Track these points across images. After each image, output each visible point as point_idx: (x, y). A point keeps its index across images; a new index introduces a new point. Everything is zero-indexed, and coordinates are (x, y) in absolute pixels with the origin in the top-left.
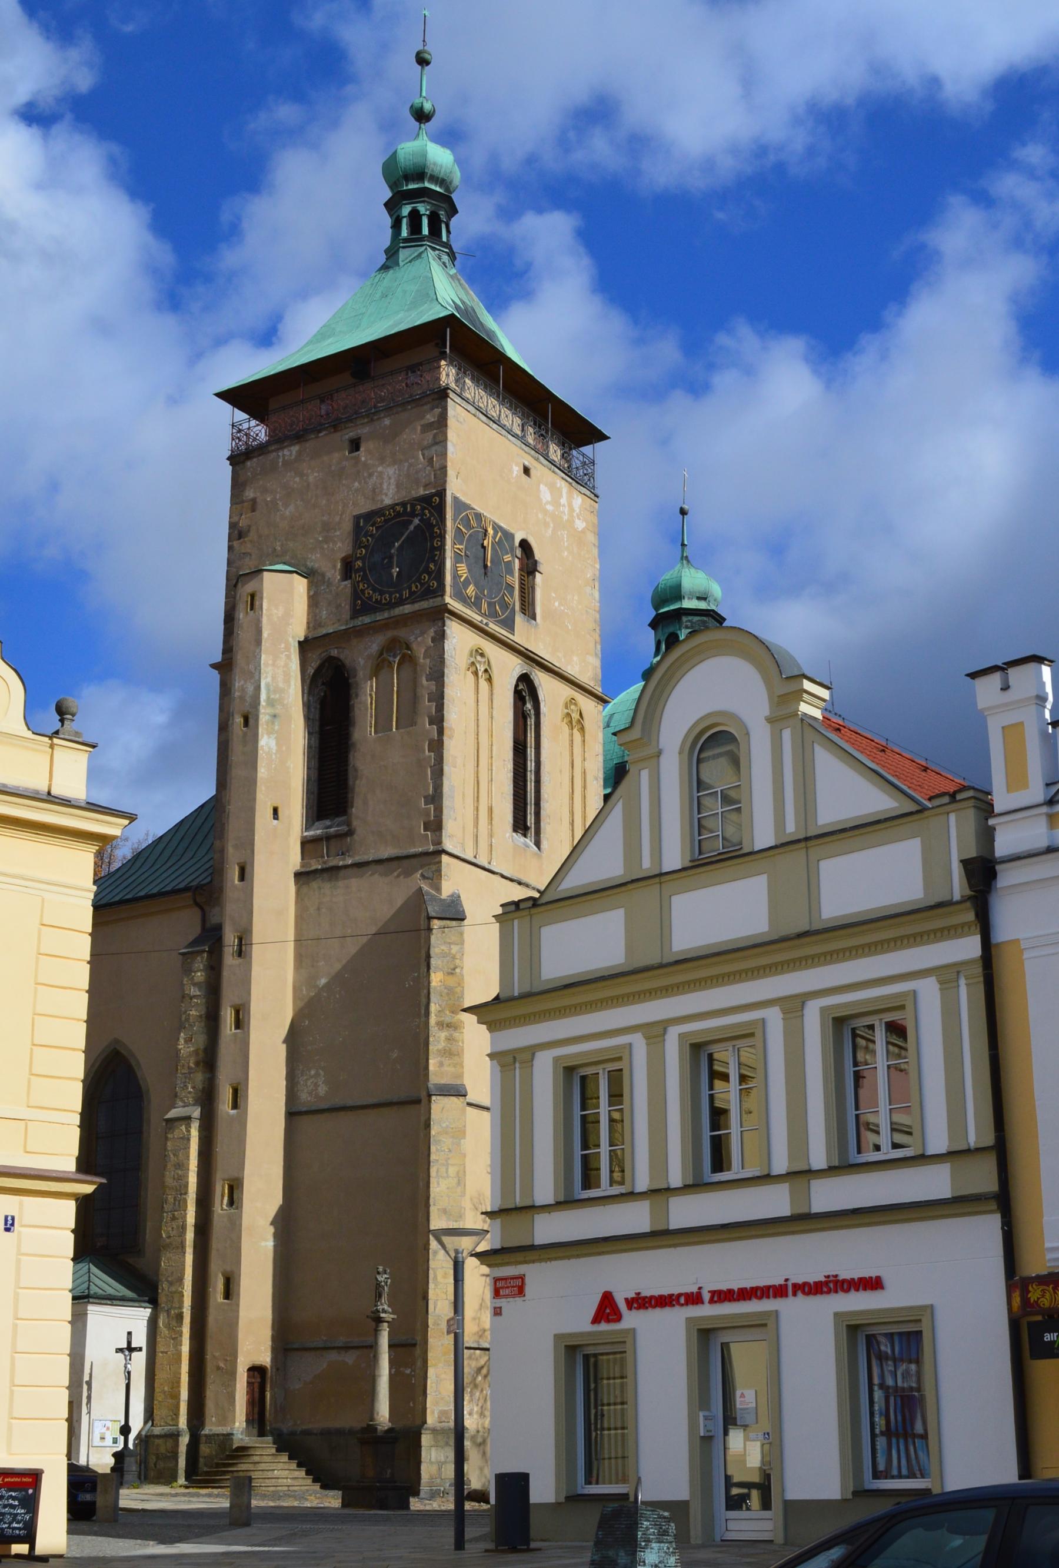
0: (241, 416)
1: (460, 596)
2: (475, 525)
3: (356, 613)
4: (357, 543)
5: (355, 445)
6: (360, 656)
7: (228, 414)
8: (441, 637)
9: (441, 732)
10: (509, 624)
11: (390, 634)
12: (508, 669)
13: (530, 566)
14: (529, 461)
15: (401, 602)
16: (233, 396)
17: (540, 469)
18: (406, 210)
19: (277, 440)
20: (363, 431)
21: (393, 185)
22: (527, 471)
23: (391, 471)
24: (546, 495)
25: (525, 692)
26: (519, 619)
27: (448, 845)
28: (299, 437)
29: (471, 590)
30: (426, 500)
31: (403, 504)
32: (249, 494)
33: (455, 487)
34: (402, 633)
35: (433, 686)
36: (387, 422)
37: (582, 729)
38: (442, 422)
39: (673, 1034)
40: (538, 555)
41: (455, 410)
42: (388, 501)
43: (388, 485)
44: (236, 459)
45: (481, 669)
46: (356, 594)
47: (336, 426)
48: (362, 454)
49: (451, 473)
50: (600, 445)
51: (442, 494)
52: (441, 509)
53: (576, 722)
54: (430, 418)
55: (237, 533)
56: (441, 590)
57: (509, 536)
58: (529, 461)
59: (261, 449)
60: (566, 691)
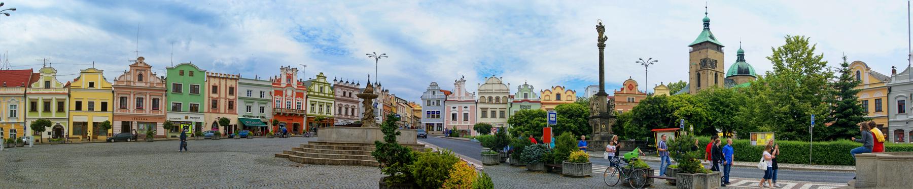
25: (716, 75)
43: (703, 57)
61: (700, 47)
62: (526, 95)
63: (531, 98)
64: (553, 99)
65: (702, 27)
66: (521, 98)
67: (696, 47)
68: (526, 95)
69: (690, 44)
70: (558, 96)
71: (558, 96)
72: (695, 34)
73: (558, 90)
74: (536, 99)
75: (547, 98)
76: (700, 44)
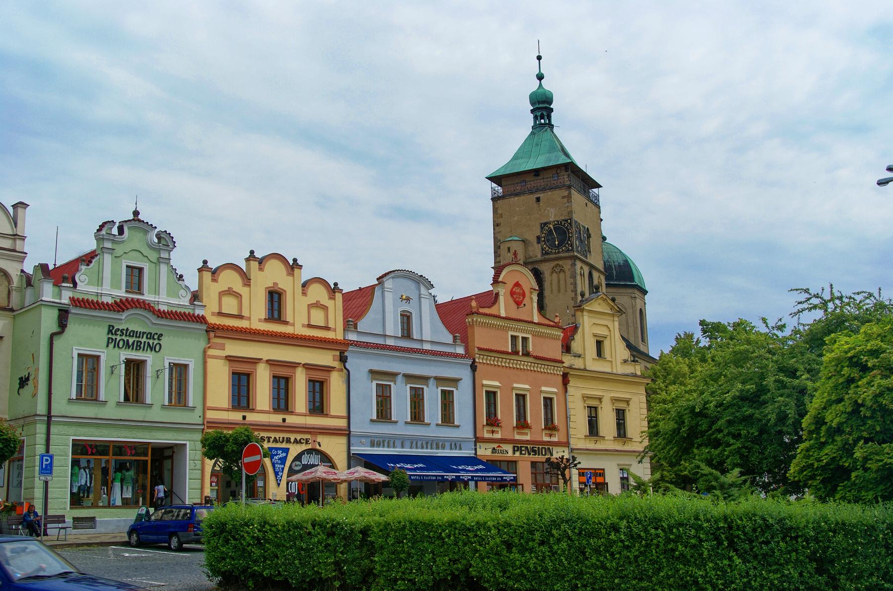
0: (494, 185)
1: (578, 252)
2: (578, 225)
3: (543, 254)
5: (538, 199)
6: (546, 268)
7: (489, 185)
10: (586, 257)
11: (556, 262)
13: (589, 236)
15: (559, 252)
16: (492, 179)
18: (539, 114)
20: (541, 195)
21: (532, 104)
28: (517, 195)
30: (567, 221)
32: (500, 212)
33: (575, 217)
34: (560, 263)
35: (572, 280)
42: (552, 220)
43: (553, 215)
44: (495, 199)
46: (543, 249)
47: (531, 193)
52: (570, 224)
55: (496, 225)
56: (572, 250)
61: (539, 182)
62: (135, 275)
63: (163, 297)
64: (256, 315)
65: (530, 120)
66: (113, 289)
67: (509, 184)
68: (135, 275)
69: (492, 170)
70: (275, 298)
71: (275, 298)
72: (507, 141)
73: (274, 275)
74: (182, 301)
75: (230, 305)
76: (536, 172)
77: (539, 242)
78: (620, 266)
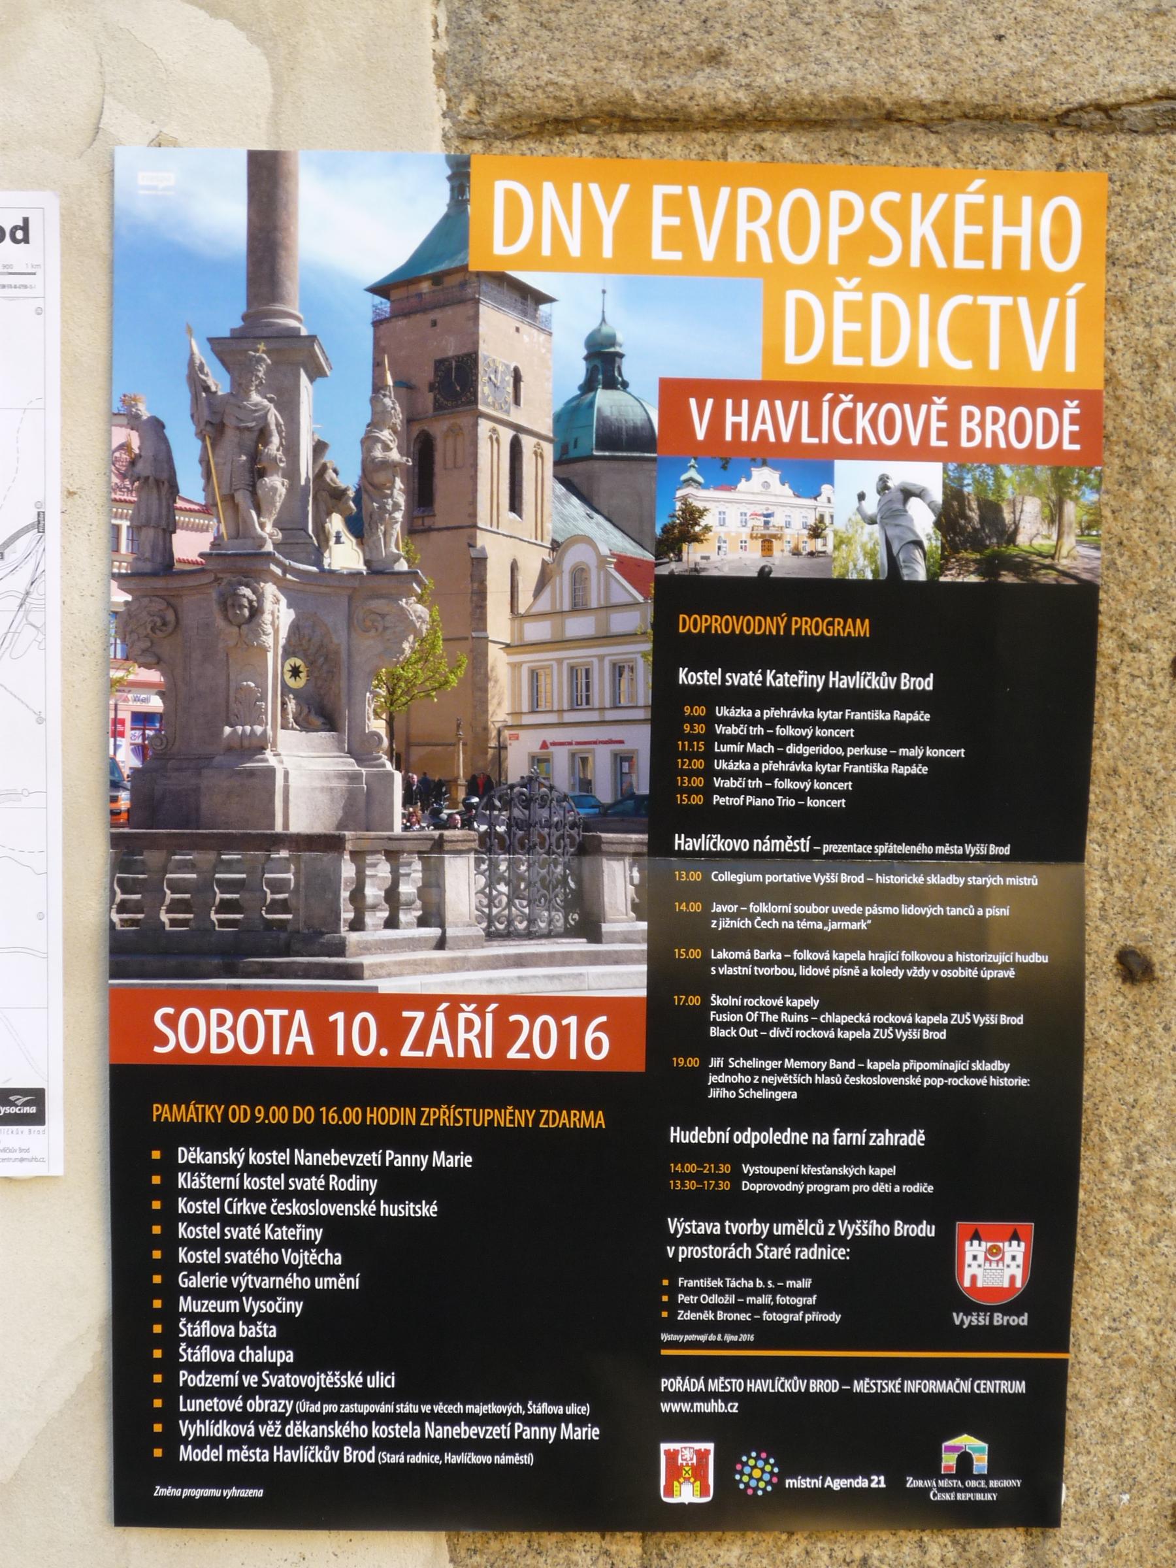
4: (436, 375)
6: (438, 429)
8: (476, 425)
9: (476, 471)
10: (508, 412)
12: (506, 435)
14: (518, 324)
17: (524, 328)
19: (396, 314)
22: (517, 330)
23: (451, 339)
24: (526, 339)
26: (513, 408)
27: (480, 525)
29: (490, 400)
30: (469, 355)
31: (458, 357)
32: (383, 343)
33: (484, 350)
36: (450, 312)
37: (542, 457)
38: (476, 318)
39: (565, 663)
40: (522, 373)
41: (483, 309)
42: (451, 354)
43: (452, 348)
44: (377, 324)
45: (494, 437)
48: (438, 329)
49: (481, 342)
50: (554, 304)
51: (476, 353)
53: (539, 455)
54: (471, 313)
57: (507, 366)
58: (518, 324)
59: (386, 320)
60: (535, 440)
77: (431, 391)
78: (635, 428)
